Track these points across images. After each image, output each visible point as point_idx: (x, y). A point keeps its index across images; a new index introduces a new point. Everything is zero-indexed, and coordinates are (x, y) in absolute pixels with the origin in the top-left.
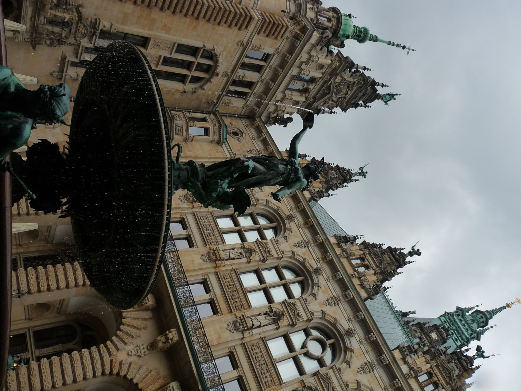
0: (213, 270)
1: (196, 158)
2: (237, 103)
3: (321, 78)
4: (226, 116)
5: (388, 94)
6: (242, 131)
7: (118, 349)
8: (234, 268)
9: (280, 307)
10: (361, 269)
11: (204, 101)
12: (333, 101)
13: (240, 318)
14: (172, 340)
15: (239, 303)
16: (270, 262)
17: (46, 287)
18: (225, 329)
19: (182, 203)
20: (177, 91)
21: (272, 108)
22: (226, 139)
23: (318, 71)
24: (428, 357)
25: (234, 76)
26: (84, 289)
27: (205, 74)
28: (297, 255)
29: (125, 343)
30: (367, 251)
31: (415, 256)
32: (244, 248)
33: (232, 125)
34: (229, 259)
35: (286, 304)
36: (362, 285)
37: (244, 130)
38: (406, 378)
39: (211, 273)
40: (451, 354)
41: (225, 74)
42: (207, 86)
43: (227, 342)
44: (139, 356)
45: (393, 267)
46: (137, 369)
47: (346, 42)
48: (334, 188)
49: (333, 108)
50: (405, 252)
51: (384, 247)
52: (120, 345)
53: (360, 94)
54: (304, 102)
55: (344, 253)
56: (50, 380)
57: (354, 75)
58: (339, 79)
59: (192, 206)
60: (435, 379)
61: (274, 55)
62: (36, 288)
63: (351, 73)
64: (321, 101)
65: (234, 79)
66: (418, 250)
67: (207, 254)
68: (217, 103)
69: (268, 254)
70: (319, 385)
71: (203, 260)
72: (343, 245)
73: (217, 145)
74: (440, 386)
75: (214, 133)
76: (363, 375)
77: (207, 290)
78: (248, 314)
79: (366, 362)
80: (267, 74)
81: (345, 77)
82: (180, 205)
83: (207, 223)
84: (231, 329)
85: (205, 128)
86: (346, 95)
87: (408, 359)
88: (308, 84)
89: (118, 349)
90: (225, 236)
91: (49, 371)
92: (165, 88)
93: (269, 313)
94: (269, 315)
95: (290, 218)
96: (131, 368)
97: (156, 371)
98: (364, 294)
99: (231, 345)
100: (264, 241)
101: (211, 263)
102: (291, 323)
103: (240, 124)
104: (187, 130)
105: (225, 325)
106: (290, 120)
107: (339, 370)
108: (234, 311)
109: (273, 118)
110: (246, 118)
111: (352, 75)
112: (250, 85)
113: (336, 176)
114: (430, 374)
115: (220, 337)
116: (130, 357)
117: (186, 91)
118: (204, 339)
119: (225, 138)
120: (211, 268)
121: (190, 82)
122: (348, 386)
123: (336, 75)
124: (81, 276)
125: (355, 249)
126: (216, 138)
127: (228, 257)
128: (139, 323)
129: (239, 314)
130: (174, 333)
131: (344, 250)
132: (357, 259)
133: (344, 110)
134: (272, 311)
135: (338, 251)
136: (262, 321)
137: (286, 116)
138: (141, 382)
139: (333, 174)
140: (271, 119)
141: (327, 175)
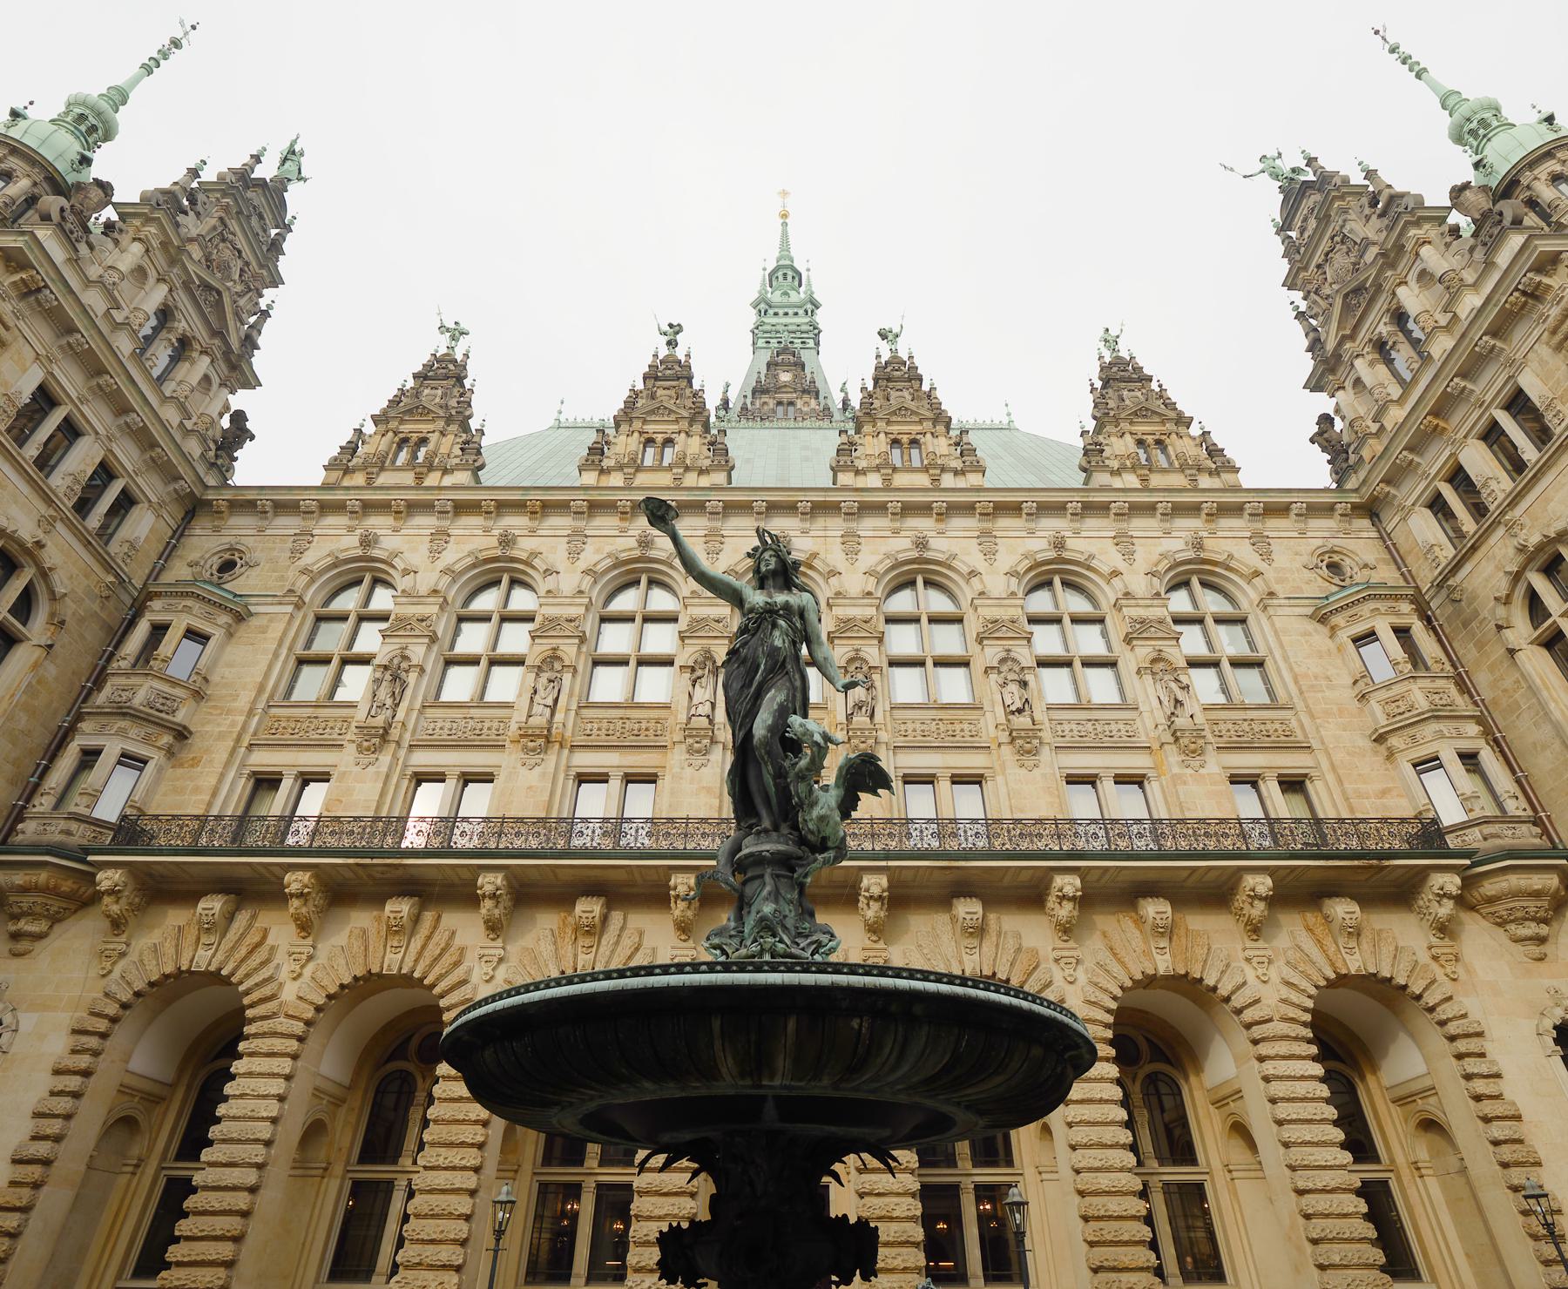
0: (566, 752)
1: (261, 689)
2: (142, 526)
3: (171, 290)
4: (163, 568)
5: (284, 161)
6: (227, 546)
8: (574, 707)
9: (690, 650)
10: (669, 455)
11: (96, 607)
12: (240, 295)
15: (652, 725)
16: (589, 626)
20: (36, 666)
21: (193, 447)
22: (236, 596)
23: (147, 288)
24: (867, 428)
25: (63, 503)
27: (18, 576)
28: (595, 565)
30: (637, 425)
31: (679, 337)
32: (539, 669)
33: (197, 564)
34: (553, 714)
36: (702, 472)
37: (226, 540)
38: (888, 488)
39: (568, 759)
40: (875, 387)
41: (47, 523)
42: (59, 583)
45: (688, 391)
47: (97, 171)
48: (467, 413)
49: (257, 304)
50: (664, 352)
51: (640, 386)
53: (254, 221)
54: (212, 361)
55: (626, 470)
57: (199, 208)
58: (196, 252)
60: (905, 439)
61: (52, 374)
63: (191, 213)
64: (231, 323)
65: (70, 504)
66: (671, 326)
68: (117, 575)
70: (850, 642)
72: (606, 463)
73: (243, 626)
74: (918, 437)
75: (209, 617)
76: (860, 556)
77: (602, 778)
78: (683, 718)
79: (840, 540)
80: (96, 416)
81: (194, 233)
83: (448, 725)
85: (185, 637)
86: (240, 256)
87: (861, 464)
88: (170, 330)
90: (490, 697)
92: (13, 695)
93: (694, 676)
94: (699, 678)
95: (507, 541)
98: (719, 478)
100: (538, 619)
103: (204, 544)
104: (174, 683)
105: (689, 770)
106: (239, 418)
107: (838, 594)
109: (217, 456)
110: (189, 522)
111: (198, 214)
112: (105, 473)
113: (439, 392)
114: (895, 442)
115: (709, 790)
117: (49, 642)
118: (710, 824)
119: (231, 597)
120: (559, 754)
121: (24, 624)
122: (869, 593)
123: (180, 250)
125: (624, 444)
126: (224, 619)
129: (678, 737)
130: (679, 881)
131: (620, 467)
132: (644, 451)
133: (276, 281)
135: (616, 480)
136: (707, 697)
137: (225, 422)
139: (432, 396)
140: (219, 462)
141: (430, 411)
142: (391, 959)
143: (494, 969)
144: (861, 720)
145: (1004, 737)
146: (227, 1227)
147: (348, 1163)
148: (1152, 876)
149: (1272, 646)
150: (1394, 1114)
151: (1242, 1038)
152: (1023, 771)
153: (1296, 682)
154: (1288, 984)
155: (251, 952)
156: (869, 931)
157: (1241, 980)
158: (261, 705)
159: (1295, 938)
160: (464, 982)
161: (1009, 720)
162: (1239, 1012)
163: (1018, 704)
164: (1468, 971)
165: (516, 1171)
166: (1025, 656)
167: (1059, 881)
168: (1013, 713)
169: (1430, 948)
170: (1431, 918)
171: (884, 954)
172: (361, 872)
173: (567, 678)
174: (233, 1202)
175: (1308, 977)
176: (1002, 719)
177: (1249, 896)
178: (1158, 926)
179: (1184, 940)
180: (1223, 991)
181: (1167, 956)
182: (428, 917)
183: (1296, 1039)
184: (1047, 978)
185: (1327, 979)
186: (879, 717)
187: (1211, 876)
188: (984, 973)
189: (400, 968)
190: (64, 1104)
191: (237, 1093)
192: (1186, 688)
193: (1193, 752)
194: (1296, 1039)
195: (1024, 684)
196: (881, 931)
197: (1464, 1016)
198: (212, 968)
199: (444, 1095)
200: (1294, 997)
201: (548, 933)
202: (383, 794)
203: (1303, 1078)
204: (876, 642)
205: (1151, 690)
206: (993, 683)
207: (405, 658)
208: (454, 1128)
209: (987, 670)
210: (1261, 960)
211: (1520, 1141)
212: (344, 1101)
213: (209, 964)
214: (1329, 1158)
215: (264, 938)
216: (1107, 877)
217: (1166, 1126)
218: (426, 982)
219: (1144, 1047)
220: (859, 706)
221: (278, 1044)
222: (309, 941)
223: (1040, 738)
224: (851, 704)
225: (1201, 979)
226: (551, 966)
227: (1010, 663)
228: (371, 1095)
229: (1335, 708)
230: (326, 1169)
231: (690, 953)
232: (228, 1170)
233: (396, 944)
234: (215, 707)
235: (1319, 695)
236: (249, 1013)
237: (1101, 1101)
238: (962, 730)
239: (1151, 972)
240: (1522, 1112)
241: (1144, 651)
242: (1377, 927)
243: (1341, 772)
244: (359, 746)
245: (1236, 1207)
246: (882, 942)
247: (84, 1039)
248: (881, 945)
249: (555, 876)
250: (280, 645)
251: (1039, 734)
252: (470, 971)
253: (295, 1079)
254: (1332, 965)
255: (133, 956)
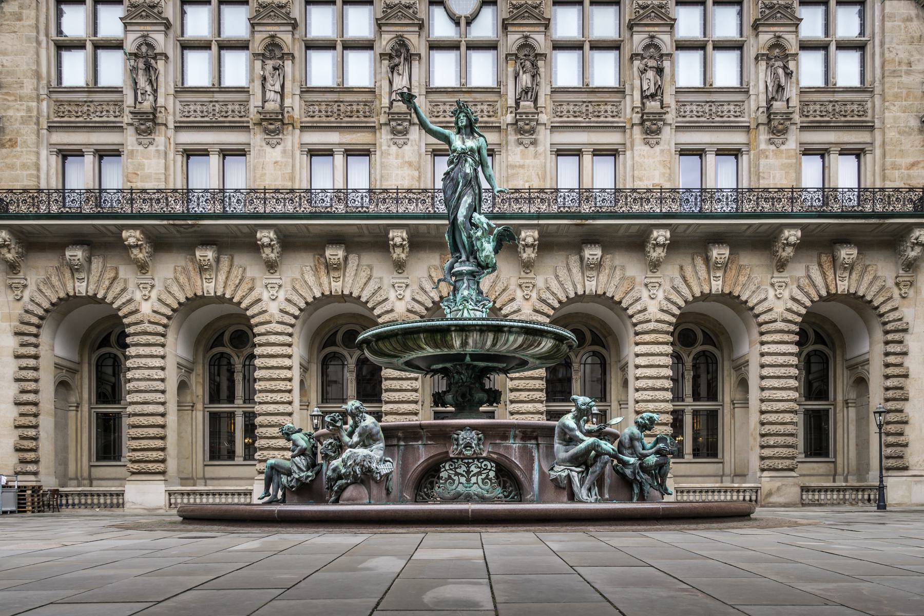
7: (392, 311)
13: (389, 120)
14: (404, 240)
17: (289, 383)
18: (400, 150)
19: (155, 144)
26: (295, 336)
29: (386, 299)
35: (383, 21)
43: (420, 155)
44: (407, 286)
46: (420, 292)
52: (386, 306)
56: (409, 394)
59: (163, 128)
62: (287, 394)
67: (268, 134)
69: (284, 11)
70: (521, 29)
71: (278, 146)
78: (385, 102)
82: (159, 148)
84: (401, 142)
89: (392, 311)
91: (399, 393)
94: (397, 65)
96: (420, 300)
97: (433, 270)
99: (423, 150)
101: (285, 132)
102: (417, 29)
105: (394, 148)
108: (374, 122)
115: (410, 164)
116: (405, 298)
124: (278, 336)
127: (279, 96)
128: (363, 276)
134: (391, 57)
138: (440, 292)
142: (207, 287)
143: (277, 292)
144: (527, 105)
145: (636, 118)
146: (156, 433)
147: (204, 404)
148: (722, 229)
149: (876, 31)
150: (845, 375)
151: (755, 331)
152: (647, 148)
153: (883, 67)
154: (794, 299)
155: (112, 283)
156: (524, 267)
157: (763, 297)
158: (43, 91)
159: (808, 271)
160: (259, 300)
161: (643, 104)
162: (757, 316)
163: (652, 90)
164: (916, 292)
165: (308, 406)
166: (666, 41)
167: (655, 233)
168: (647, 97)
169: (896, 278)
170: (904, 258)
171: (533, 281)
172: (172, 229)
173: (288, 64)
174: (154, 421)
175: (807, 295)
176: (638, 103)
177: (783, 243)
178: (717, 263)
179: (733, 272)
180: (750, 304)
181: (720, 282)
182: (225, 261)
183: (789, 332)
184: (638, 295)
185: (820, 296)
186: (541, 102)
187: (762, 229)
188: (598, 293)
189: (215, 293)
190: (31, 374)
191: (135, 366)
192: (789, 74)
193: (779, 132)
194: (789, 332)
195: (660, 71)
196: (532, 266)
197: (900, 320)
198: (91, 293)
199: (261, 366)
200: (795, 307)
201: (308, 268)
202: (166, 168)
203: (784, 354)
204: (543, 29)
205: (762, 76)
206: (635, 69)
207: (150, 46)
208: (273, 383)
209: (633, 57)
210: (780, 284)
211: (901, 388)
212: (193, 370)
213: (87, 292)
214: (785, 395)
215: (117, 273)
216: (691, 229)
217: (708, 381)
218: (235, 300)
219: (700, 336)
220: (526, 91)
221: (152, 339)
222: (148, 275)
223: (663, 120)
224: (519, 90)
225: (739, 296)
226: (315, 290)
227: (652, 50)
228: (207, 367)
229: (904, 91)
230: (193, 406)
231: (405, 281)
232: (145, 406)
233: (209, 277)
234: (7, 94)
235: (896, 80)
236: (126, 321)
237: (659, 366)
238: (606, 111)
239: (707, 291)
240: (910, 373)
241: (765, 38)
242: (867, 263)
243: (887, 148)
244: (137, 129)
245: (732, 421)
246: (533, 272)
247: (26, 338)
248: (531, 275)
249: (308, 229)
250: (38, 33)
251: (664, 117)
252: (261, 294)
253: (167, 357)
254: (827, 287)
255: (32, 287)
